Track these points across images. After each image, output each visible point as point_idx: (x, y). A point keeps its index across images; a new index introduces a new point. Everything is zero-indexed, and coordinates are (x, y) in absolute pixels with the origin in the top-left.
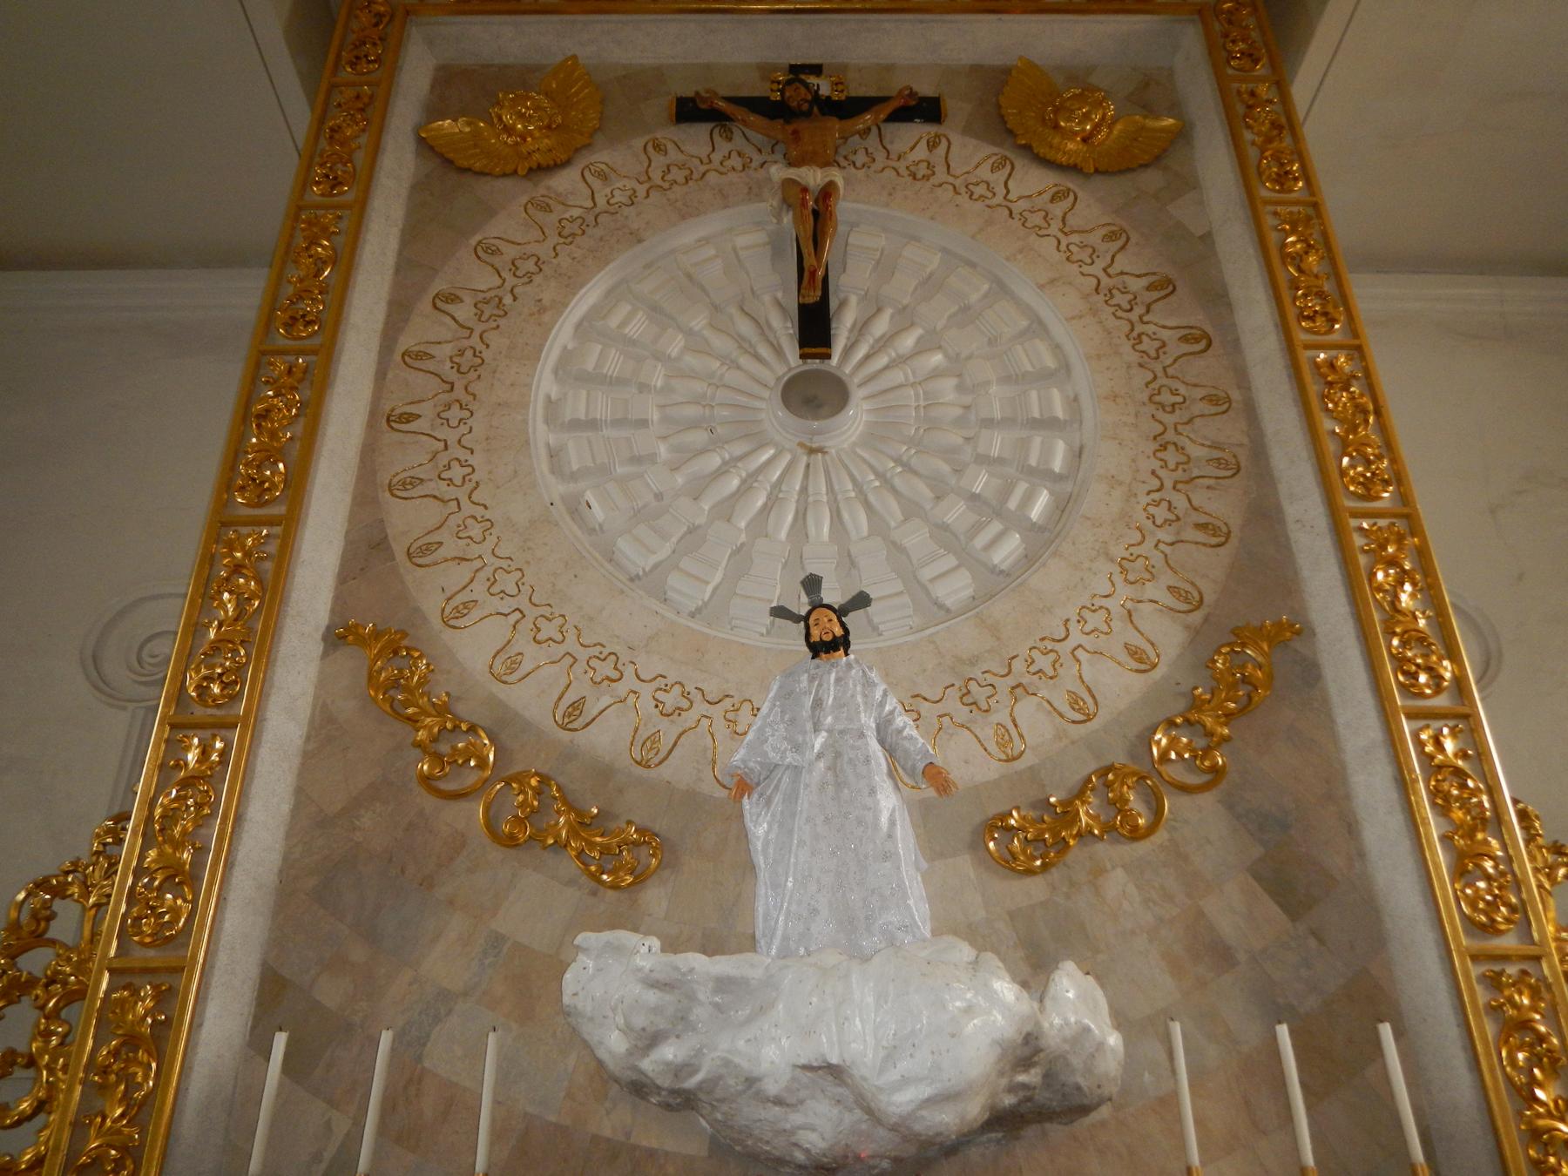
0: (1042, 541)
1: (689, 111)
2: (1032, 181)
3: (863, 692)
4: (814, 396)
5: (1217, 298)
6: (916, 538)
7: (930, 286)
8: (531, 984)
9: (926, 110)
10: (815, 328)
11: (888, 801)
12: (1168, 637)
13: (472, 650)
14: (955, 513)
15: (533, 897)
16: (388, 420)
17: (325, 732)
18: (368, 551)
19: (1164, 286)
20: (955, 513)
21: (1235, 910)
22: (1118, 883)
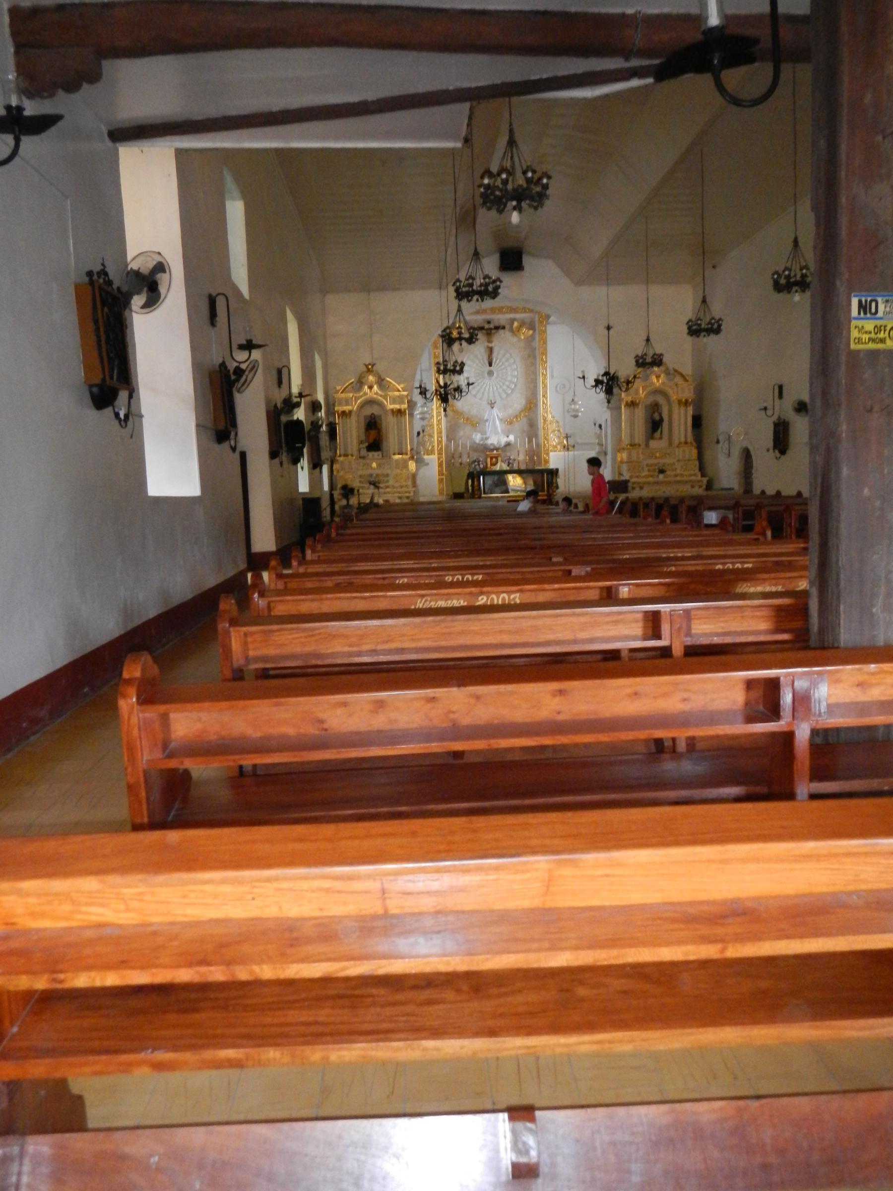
0: (513, 390)
2: (515, 339)
3: (495, 411)
4: (490, 373)
5: (535, 357)
6: (501, 391)
7: (504, 356)
9: (504, 328)
10: (490, 365)
11: (498, 422)
12: (523, 402)
14: (505, 387)
15: (468, 429)
19: (529, 356)
20: (505, 387)
21: (526, 427)
22: (517, 426)
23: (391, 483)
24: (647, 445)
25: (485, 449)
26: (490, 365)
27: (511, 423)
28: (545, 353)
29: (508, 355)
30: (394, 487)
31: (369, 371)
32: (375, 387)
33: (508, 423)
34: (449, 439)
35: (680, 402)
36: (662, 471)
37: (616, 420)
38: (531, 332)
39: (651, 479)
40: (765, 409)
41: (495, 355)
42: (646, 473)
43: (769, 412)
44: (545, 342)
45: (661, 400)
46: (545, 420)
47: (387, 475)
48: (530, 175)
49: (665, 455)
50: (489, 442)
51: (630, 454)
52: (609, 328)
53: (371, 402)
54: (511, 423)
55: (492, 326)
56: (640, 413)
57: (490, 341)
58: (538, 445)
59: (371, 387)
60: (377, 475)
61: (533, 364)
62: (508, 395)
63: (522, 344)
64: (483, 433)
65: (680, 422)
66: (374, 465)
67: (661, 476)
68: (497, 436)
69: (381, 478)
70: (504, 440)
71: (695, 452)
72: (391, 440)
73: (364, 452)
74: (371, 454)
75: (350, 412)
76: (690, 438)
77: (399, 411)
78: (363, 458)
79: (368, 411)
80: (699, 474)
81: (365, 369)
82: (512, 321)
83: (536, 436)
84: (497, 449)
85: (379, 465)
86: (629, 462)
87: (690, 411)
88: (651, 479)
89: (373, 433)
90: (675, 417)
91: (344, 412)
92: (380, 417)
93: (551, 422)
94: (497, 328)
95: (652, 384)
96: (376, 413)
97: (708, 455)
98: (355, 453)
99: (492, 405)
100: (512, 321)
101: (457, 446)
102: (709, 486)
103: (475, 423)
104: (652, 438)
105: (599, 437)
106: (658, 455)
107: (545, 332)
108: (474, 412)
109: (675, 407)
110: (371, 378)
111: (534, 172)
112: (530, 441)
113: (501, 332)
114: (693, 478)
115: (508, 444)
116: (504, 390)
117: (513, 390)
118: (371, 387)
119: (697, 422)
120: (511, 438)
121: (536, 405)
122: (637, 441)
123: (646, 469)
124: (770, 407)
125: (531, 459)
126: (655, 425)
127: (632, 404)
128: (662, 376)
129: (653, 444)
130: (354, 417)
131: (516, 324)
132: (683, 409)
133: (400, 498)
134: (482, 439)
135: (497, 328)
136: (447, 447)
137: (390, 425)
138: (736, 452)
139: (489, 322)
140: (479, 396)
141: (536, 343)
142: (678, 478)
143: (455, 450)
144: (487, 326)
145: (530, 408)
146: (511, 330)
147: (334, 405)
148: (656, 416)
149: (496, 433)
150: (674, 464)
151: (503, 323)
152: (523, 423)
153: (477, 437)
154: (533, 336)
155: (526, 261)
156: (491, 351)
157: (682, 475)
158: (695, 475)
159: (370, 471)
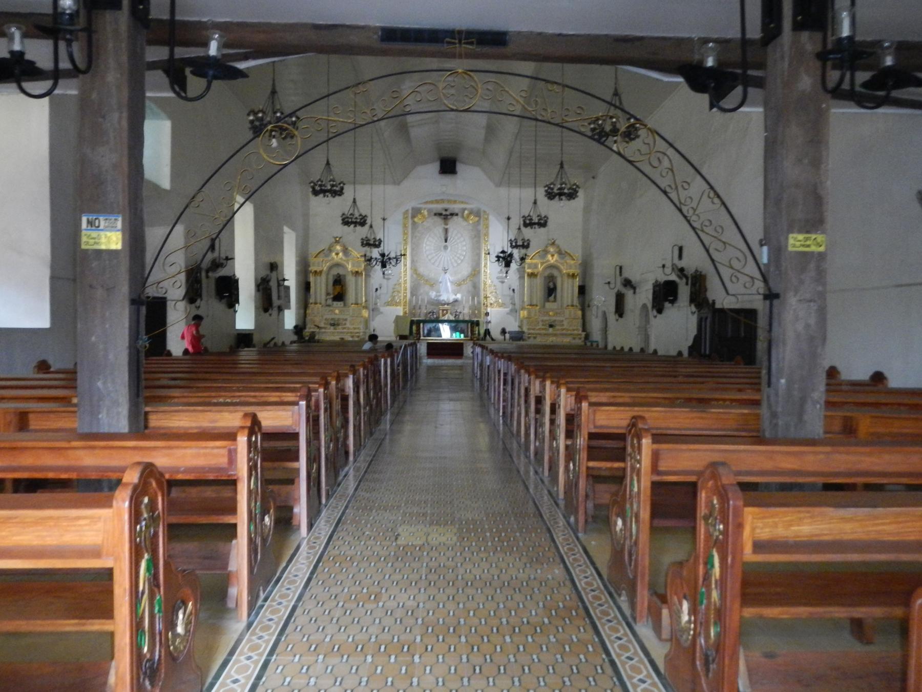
0: (462, 261)
1: (435, 214)
2: (465, 223)
3: (448, 276)
4: (446, 248)
5: (479, 237)
8: (427, 294)
9: (457, 215)
10: (446, 241)
11: (449, 284)
12: (470, 270)
13: (421, 270)
15: (427, 288)
16: (413, 249)
17: (412, 276)
18: (413, 261)
21: (471, 288)
22: (464, 287)
23: (348, 325)
24: (544, 306)
25: (439, 303)
26: (446, 241)
27: (459, 285)
28: (487, 234)
29: (459, 235)
30: (349, 328)
31: (337, 242)
32: (341, 254)
33: (459, 284)
34: (412, 294)
35: (568, 275)
36: (551, 326)
37: (522, 286)
38: (477, 219)
39: (544, 332)
40: (609, 283)
41: (449, 234)
42: (540, 326)
43: (612, 286)
44: (487, 227)
45: (555, 273)
46: (485, 284)
47: (346, 320)
48: (278, 115)
49: (556, 314)
50: (441, 298)
51: (529, 313)
52: (509, 219)
53: (337, 265)
54: (459, 285)
55: (448, 213)
56: (539, 282)
57: (446, 224)
58: (479, 303)
59: (337, 254)
60: (339, 319)
61: (479, 242)
62: (458, 264)
63: (470, 227)
64: (438, 291)
65: (568, 290)
66: (337, 311)
67: (551, 330)
68: (448, 292)
69: (341, 322)
70: (452, 298)
71: (580, 313)
72: (351, 296)
73: (330, 302)
74: (335, 303)
75: (321, 272)
76: (576, 302)
77: (357, 272)
78: (329, 306)
79: (335, 272)
80: (581, 329)
81: (333, 240)
82: (464, 209)
83: (479, 296)
84: (448, 304)
85: (340, 312)
86: (528, 318)
87: (577, 282)
88: (544, 332)
89: (338, 288)
90: (566, 285)
91: (316, 272)
92: (344, 276)
93: (490, 286)
94: (452, 215)
95: (548, 261)
96: (341, 273)
97: (588, 314)
98: (323, 302)
99: (445, 271)
100: (464, 209)
101: (417, 300)
102: (587, 337)
103: (433, 284)
104: (549, 301)
105: (512, 298)
106: (551, 313)
107: (487, 219)
108: (432, 275)
109: (565, 278)
110: (338, 248)
111: (282, 113)
112: (473, 299)
113: (455, 218)
114: (576, 332)
115: (456, 301)
116: (456, 261)
117: (462, 261)
118: (337, 254)
119: (582, 290)
120: (459, 296)
121: (479, 272)
122: (535, 303)
123: (541, 323)
124: (613, 282)
125: (473, 313)
126: (551, 291)
127: (532, 275)
128: (556, 256)
129: (548, 305)
130: (324, 277)
131: (466, 212)
132: (570, 280)
133: (352, 337)
134: (436, 296)
135: (452, 215)
136: (411, 301)
137: (351, 281)
138: (600, 314)
139: (446, 210)
140: (437, 264)
141: (481, 227)
142: (564, 332)
143: (417, 303)
144: (444, 213)
145: (474, 275)
146: (463, 217)
147: (309, 266)
148: (551, 285)
149: (448, 292)
150: (562, 321)
151: (456, 211)
152: (468, 286)
153: (433, 294)
154: (479, 221)
155: (460, 167)
156: (446, 231)
157: (568, 330)
158: (577, 330)
159: (333, 316)
